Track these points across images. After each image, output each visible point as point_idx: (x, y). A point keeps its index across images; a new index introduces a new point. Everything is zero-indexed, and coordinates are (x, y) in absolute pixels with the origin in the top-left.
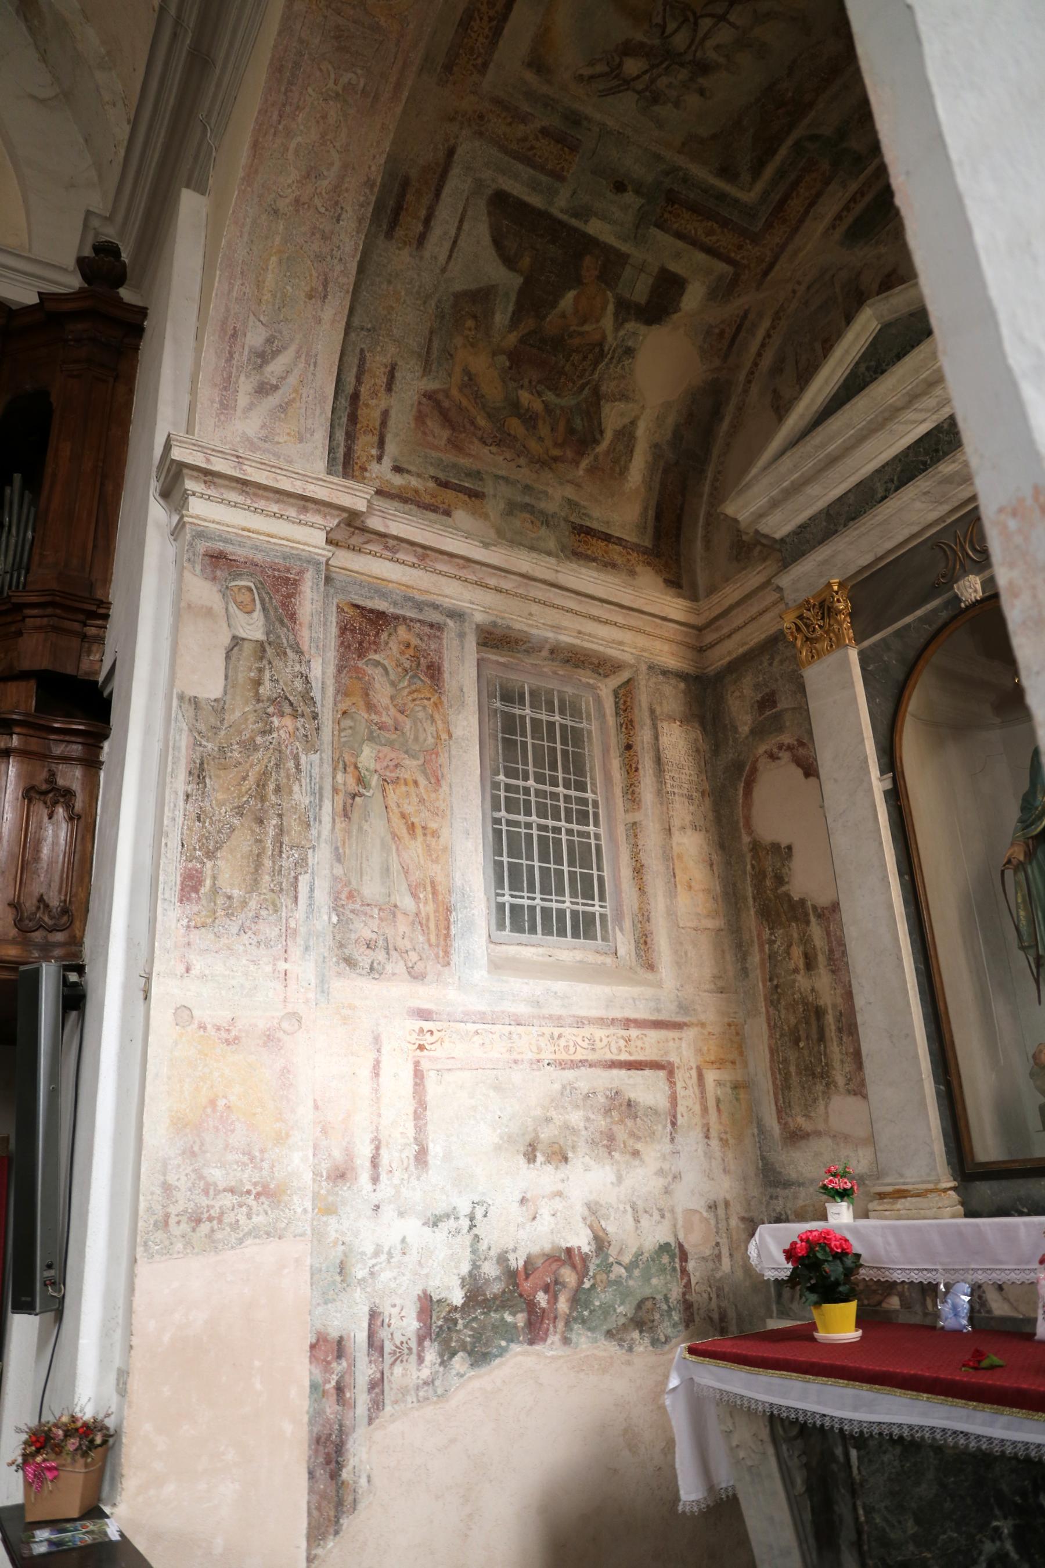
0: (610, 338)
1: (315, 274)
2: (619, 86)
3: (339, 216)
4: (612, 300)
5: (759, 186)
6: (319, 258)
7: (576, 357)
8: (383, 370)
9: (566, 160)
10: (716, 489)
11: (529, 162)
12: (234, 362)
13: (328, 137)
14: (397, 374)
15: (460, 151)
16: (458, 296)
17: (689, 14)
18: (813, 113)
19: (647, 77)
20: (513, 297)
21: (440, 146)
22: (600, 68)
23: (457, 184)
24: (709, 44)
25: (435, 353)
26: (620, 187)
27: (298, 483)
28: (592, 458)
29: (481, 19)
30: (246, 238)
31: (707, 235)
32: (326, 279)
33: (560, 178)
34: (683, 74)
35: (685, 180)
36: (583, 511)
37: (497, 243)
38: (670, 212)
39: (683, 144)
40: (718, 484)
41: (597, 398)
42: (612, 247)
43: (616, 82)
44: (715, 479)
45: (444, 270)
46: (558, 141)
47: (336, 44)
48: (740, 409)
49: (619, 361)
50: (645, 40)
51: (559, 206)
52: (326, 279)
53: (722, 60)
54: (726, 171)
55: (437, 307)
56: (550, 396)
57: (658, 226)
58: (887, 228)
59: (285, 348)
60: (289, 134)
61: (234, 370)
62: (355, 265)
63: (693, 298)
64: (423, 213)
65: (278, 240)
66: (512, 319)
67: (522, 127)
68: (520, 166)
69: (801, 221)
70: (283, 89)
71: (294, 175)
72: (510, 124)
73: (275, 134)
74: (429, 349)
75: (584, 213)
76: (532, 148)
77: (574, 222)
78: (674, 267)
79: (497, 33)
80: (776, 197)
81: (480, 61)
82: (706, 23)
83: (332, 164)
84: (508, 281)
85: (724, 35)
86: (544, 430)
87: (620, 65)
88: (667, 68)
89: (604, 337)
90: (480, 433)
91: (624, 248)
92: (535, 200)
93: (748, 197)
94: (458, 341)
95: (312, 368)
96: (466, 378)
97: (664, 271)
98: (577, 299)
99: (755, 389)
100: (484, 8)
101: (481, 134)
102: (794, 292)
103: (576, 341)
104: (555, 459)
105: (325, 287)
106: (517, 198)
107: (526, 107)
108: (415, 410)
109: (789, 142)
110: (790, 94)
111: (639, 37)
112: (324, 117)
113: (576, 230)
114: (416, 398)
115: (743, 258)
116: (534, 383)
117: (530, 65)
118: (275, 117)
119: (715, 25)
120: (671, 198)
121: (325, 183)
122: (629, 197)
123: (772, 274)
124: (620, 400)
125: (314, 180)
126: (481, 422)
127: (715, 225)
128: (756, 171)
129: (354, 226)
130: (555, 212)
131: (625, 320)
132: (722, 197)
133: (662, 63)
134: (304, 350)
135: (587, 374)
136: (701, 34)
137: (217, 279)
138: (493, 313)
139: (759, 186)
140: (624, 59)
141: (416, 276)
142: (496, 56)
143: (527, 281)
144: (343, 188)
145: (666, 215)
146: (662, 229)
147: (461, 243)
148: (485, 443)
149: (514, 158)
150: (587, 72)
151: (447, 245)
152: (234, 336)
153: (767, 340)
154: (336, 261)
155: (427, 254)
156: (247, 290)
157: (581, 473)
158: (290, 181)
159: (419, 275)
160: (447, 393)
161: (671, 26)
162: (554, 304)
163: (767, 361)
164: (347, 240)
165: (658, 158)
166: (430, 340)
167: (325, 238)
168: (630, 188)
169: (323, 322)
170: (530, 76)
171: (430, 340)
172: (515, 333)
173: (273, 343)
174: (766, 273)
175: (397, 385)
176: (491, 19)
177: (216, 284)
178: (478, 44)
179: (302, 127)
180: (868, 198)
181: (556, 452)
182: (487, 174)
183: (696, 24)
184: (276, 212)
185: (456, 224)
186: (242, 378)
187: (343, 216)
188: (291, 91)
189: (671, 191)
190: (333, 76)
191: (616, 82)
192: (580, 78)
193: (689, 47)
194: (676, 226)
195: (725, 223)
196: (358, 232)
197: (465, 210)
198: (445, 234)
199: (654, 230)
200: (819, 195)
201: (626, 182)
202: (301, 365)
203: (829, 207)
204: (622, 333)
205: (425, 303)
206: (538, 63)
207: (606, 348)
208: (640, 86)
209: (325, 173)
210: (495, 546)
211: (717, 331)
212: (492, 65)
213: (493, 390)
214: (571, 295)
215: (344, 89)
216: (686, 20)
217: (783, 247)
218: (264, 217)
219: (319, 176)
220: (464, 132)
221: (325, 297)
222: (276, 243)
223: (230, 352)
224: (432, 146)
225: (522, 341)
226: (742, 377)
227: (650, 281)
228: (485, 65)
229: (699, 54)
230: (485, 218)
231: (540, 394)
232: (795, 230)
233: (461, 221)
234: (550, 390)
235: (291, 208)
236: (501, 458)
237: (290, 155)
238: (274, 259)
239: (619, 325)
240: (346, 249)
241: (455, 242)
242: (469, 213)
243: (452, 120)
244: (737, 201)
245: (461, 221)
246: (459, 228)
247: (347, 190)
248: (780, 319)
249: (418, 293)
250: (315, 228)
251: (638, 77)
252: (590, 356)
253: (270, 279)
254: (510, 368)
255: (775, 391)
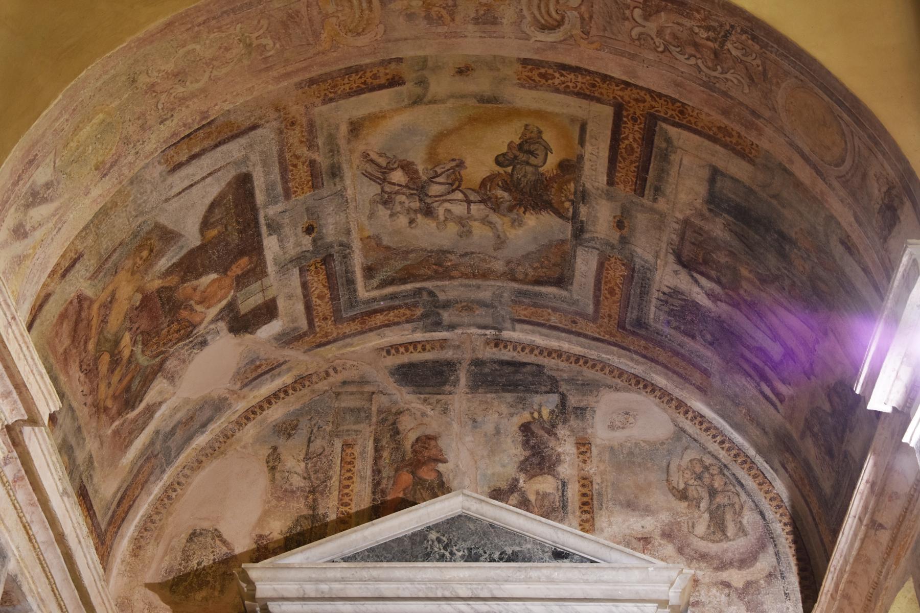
0: (203, 326)
1: (113, 151)
2: (379, 178)
3: (166, 120)
4: (229, 298)
5: (375, 293)
6: (127, 141)
7: (175, 326)
8: (73, 254)
9: (302, 189)
10: (169, 498)
11: (284, 171)
12: (17, 189)
13: (215, 63)
14: (77, 265)
15: (259, 131)
16: (157, 226)
17: (457, 183)
18: (447, 283)
19: (397, 188)
20: (184, 252)
21: (253, 119)
22: (382, 162)
23: (234, 149)
24: (447, 205)
25: (109, 264)
26: (309, 230)
27: (27, 368)
28: (122, 421)
29: (361, 77)
30: (99, 84)
31: (319, 297)
32: (116, 161)
33: (287, 194)
34: (416, 205)
35: (345, 257)
36: (92, 472)
37: (212, 206)
38: (316, 268)
39: (369, 237)
40: (174, 495)
41: (159, 369)
42: (265, 263)
43: (379, 175)
44: (171, 487)
45: (167, 200)
46: (312, 175)
47: (285, 19)
48: (226, 436)
49: (193, 347)
50: (421, 172)
51: (267, 211)
52: (116, 161)
53: (442, 218)
54: (369, 271)
55: (139, 226)
56: (138, 349)
57: (301, 270)
58: (439, 397)
59: (52, 200)
60: (196, 38)
61: (12, 197)
62: (142, 164)
63: (269, 330)
64: (197, 150)
65: (116, 103)
66: (167, 270)
67: (305, 149)
68: (276, 170)
69: (371, 330)
70: (225, 9)
71: (170, 67)
72: (302, 142)
73: (187, 30)
74: (109, 257)
75: (274, 227)
76: (295, 166)
77: (264, 230)
78: (281, 304)
79: (359, 92)
80: (375, 306)
81: (331, 95)
82: (459, 195)
83: (197, 81)
84: (192, 237)
85: (459, 209)
86: (115, 379)
87: (393, 169)
88: (412, 194)
89: (201, 323)
90: (84, 354)
91: (271, 268)
92: (260, 197)
93: (363, 293)
94: (129, 264)
95: (54, 233)
96: (109, 299)
97: (274, 300)
98: (214, 281)
99: (250, 431)
100: (369, 74)
101: (281, 133)
102: (327, 374)
103: (184, 314)
104: (106, 409)
105: (112, 166)
106: (253, 188)
107: (320, 141)
108: (65, 306)
109: (418, 285)
110: (449, 264)
111: (420, 168)
112: (227, 49)
113: (259, 235)
114: (72, 295)
115: (319, 326)
116: (139, 331)
117: (351, 123)
118: (201, 20)
119: (461, 201)
120: (327, 260)
121: (181, 89)
122: (307, 241)
123: (322, 349)
124: (168, 379)
125: (177, 81)
126: (91, 346)
127: (329, 295)
128: (384, 284)
129: (166, 135)
130: (261, 215)
131: (222, 319)
132: (351, 282)
133: (413, 189)
134: (61, 211)
135: (169, 345)
136: (449, 197)
137: (56, 101)
138: (163, 256)
139: (375, 293)
140: (399, 169)
141: (149, 191)
142: (342, 102)
143: (201, 248)
144: (187, 103)
145: (312, 268)
146: (300, 274)
147: (194, 189)
148: (81, 366)
149: (279, 163)
150: (373, 156)
151: (187, 183)
152: (31, 162)
153: (282, 395)
154: (134, 151)
155: (170, 180)
156: (66, 128)
157: (110, 432)
158: (163, 68)
159: (152, 192)
160: (92, 302)
161: (441, 179)
162: (198, 276)
163: (276, 413)
164: (154, 141)
165: (348, 232)
166: (115, 250)
167: (143, 127)
168: (313, 235)
169: (89, 195)
170: (344, 129)
171: (115, 250)
172: (160, 281)
173: (49, 189)
174: (320, 345)
175: (69, 276)
176: (365, 83)
177: (52, 106)
178: (342, 87)
179: (208, 42)
180: (428, 356)
181: (109, 403)
182: (255, 158)
183: (453, 191)
184: (134, 81)
185: (205, 174)
186: (12, 210)
187: (167, 123)
188: (228, 15)
189: (331, 255)
190: (261, 32)
191: (379, 175)
192: (366, 155)
193: (436, 196)
194: (309, 278)
195: (335, 298)
196: (164, 142)
197: (219, 170)
198: (193, 175)
199: (296, 271)
200: (398, 324)
201: (316, 230)
202: (51, 225)
203: (393, 336)
204: (212, 326)
205: (136, 216)
206: (355, 128)
207: (195, 332)
208: (388, 188)
209: (188, 83)
210: (68, 497)
211: (258, 363)
212: (333, 104)
213: (115, 320)
214: (213, 276)
215: (258, 46)
216: (452, 185)
217: (345, 336)
218: (124, 78)
219: (182, 82)
220: (274, 123)
221: (105, 175)
222: (113, 105)
223: (19, 176)
224: (249, 114)
225: (159, 291)
226: (241, 406)
227: (260, 302)
228: (331, 100)
229: (435, 204)
230: (223, 184)
231: (135, 343)
232: (362, 332)
233: (210, 174)
234: (143, 344)
235: (145, 87)
236: (81, 389)
237: (181, 52)
238: (101, 116)
239: (214, 321)
240: (147, 148)
241: (192, 186)
242: (220, 173)
243: (277, 110)
244: (355, 291)
245: (210, 174)
246: (204, 178)
247: (187, 107)
248: (304, 386)
249: (140, 205)
250: (144, 115)
251: (394, 184)
252: (182, 332)
253: (87, 130)
254: (137, 308)
255: (275, 449)
